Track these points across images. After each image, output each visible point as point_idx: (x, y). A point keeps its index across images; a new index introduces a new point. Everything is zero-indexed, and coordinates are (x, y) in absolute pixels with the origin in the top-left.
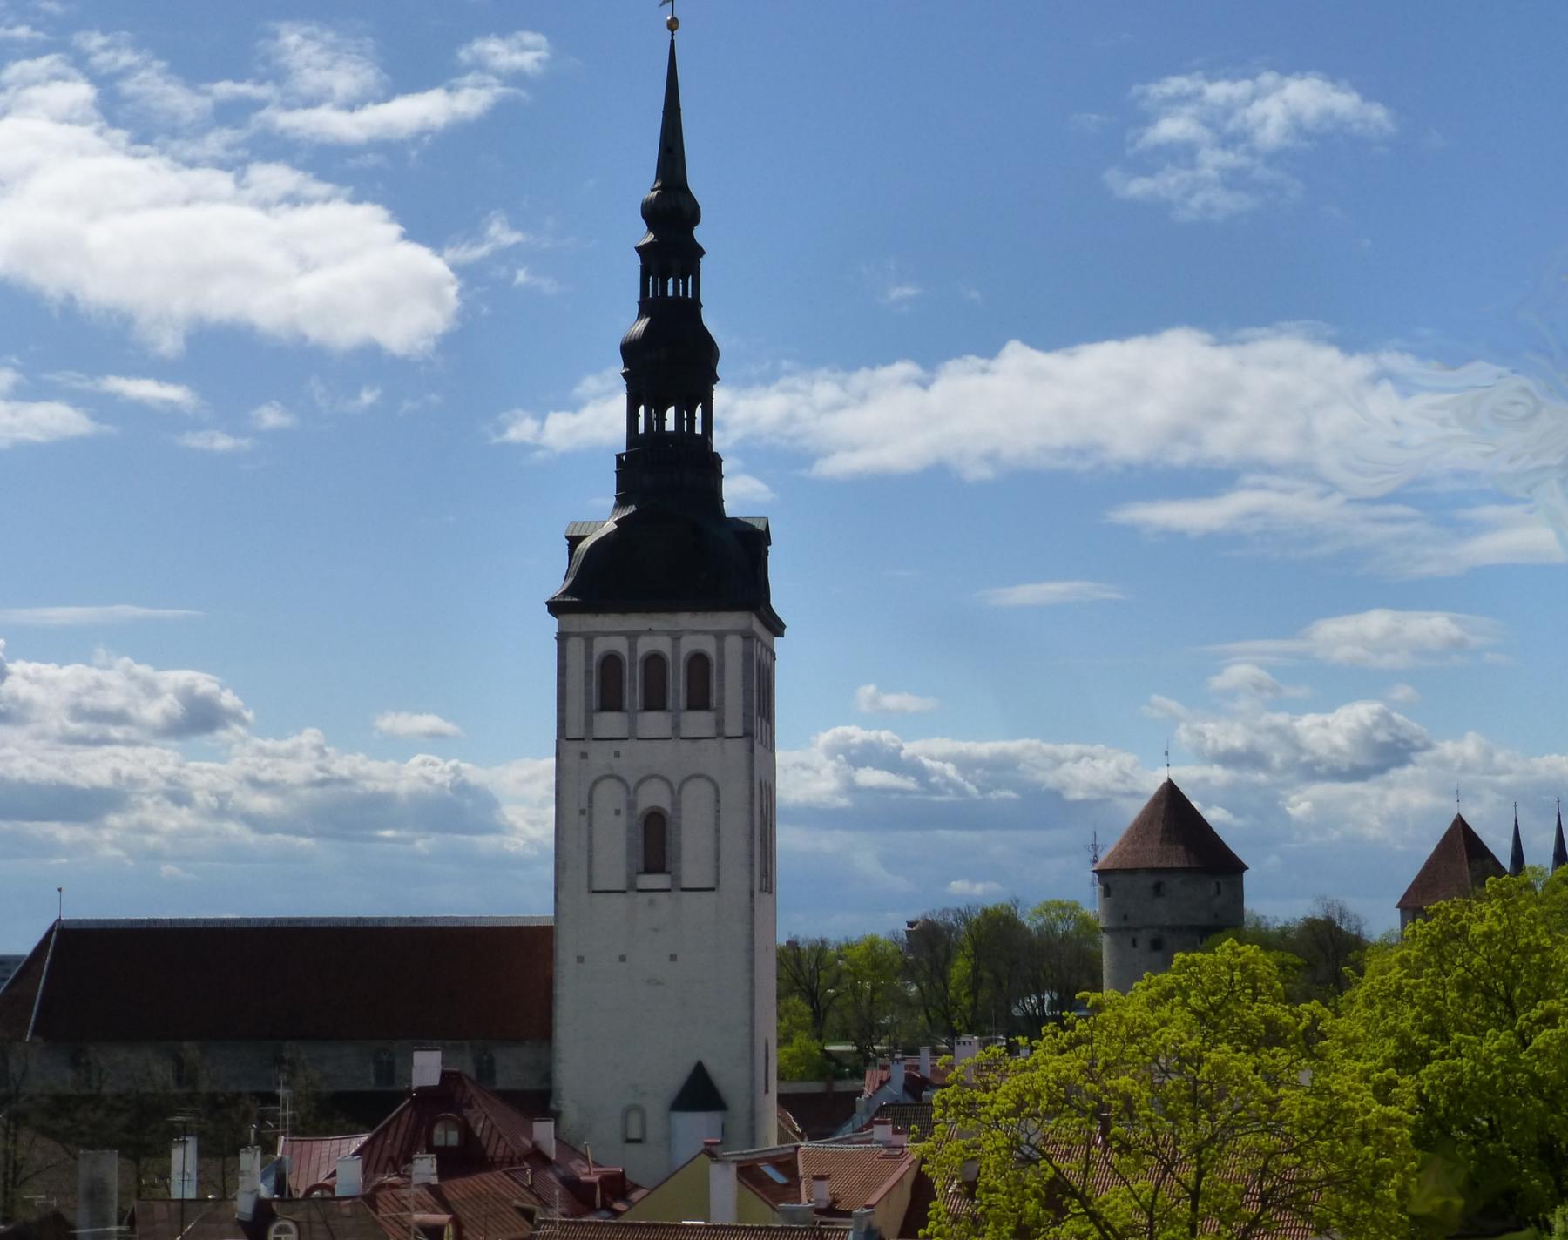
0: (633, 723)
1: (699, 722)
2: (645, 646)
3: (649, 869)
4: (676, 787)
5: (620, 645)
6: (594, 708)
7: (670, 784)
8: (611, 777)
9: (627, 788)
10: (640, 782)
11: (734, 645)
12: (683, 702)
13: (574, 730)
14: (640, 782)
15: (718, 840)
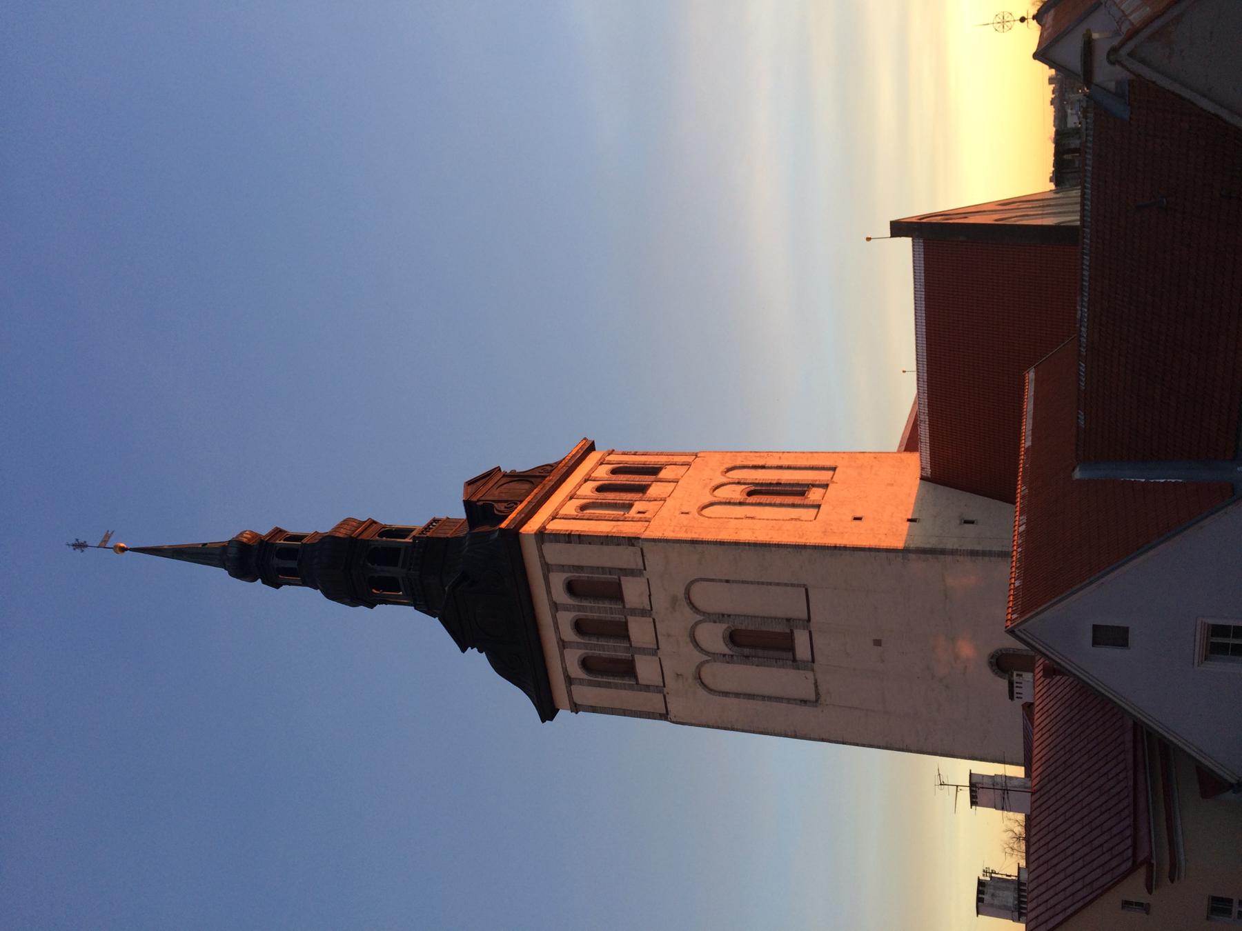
0: (643, 651)
1: (633, 591)
2: (569, 634)
3: (791, 648)
4: (702, 618)
5: (573, 658)
6: (633, 682)
7: (696, 624)
8: (699, 678)
9: (707, 661)
10: (701, 650)
11: (554, 553)
12: (617, 606)
13: (656, 703)
14: (701, 650)
15: (752, 583)
